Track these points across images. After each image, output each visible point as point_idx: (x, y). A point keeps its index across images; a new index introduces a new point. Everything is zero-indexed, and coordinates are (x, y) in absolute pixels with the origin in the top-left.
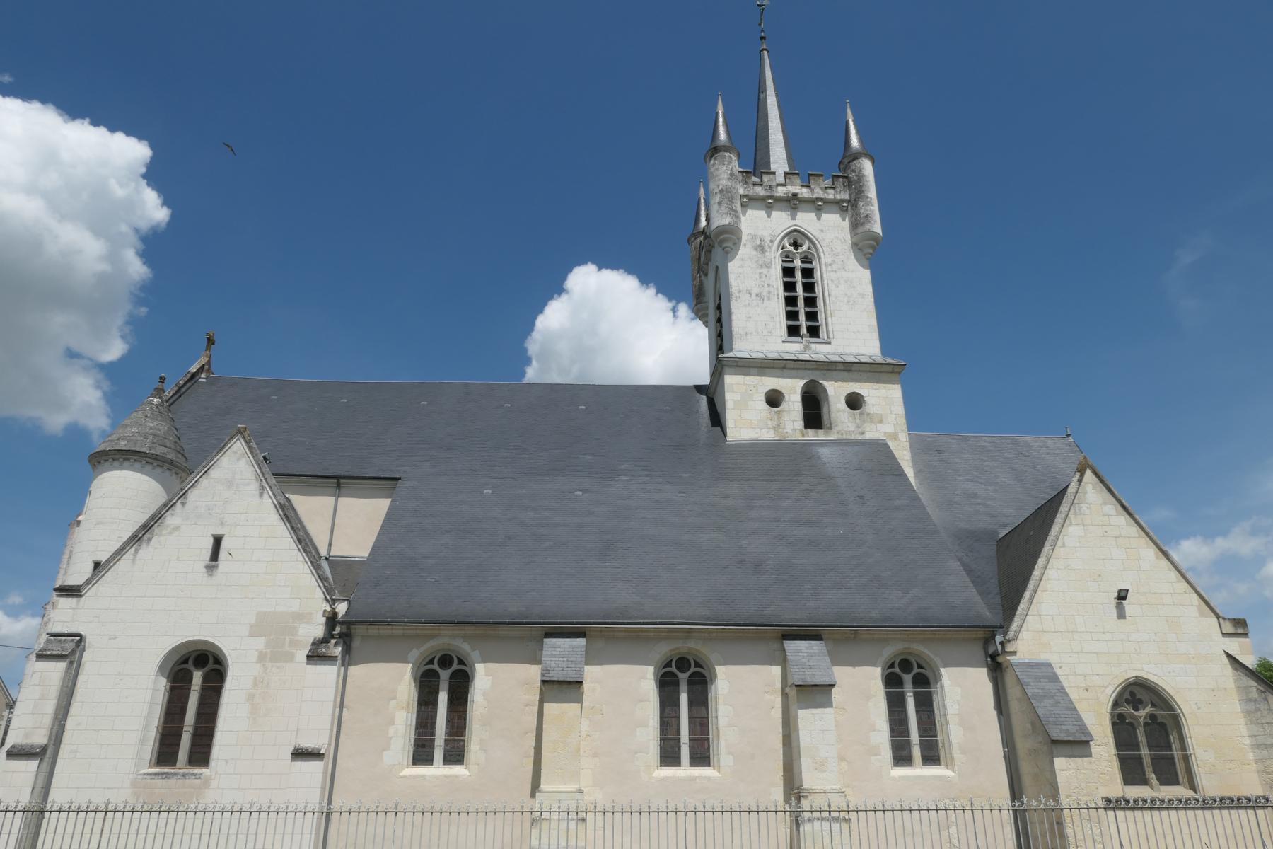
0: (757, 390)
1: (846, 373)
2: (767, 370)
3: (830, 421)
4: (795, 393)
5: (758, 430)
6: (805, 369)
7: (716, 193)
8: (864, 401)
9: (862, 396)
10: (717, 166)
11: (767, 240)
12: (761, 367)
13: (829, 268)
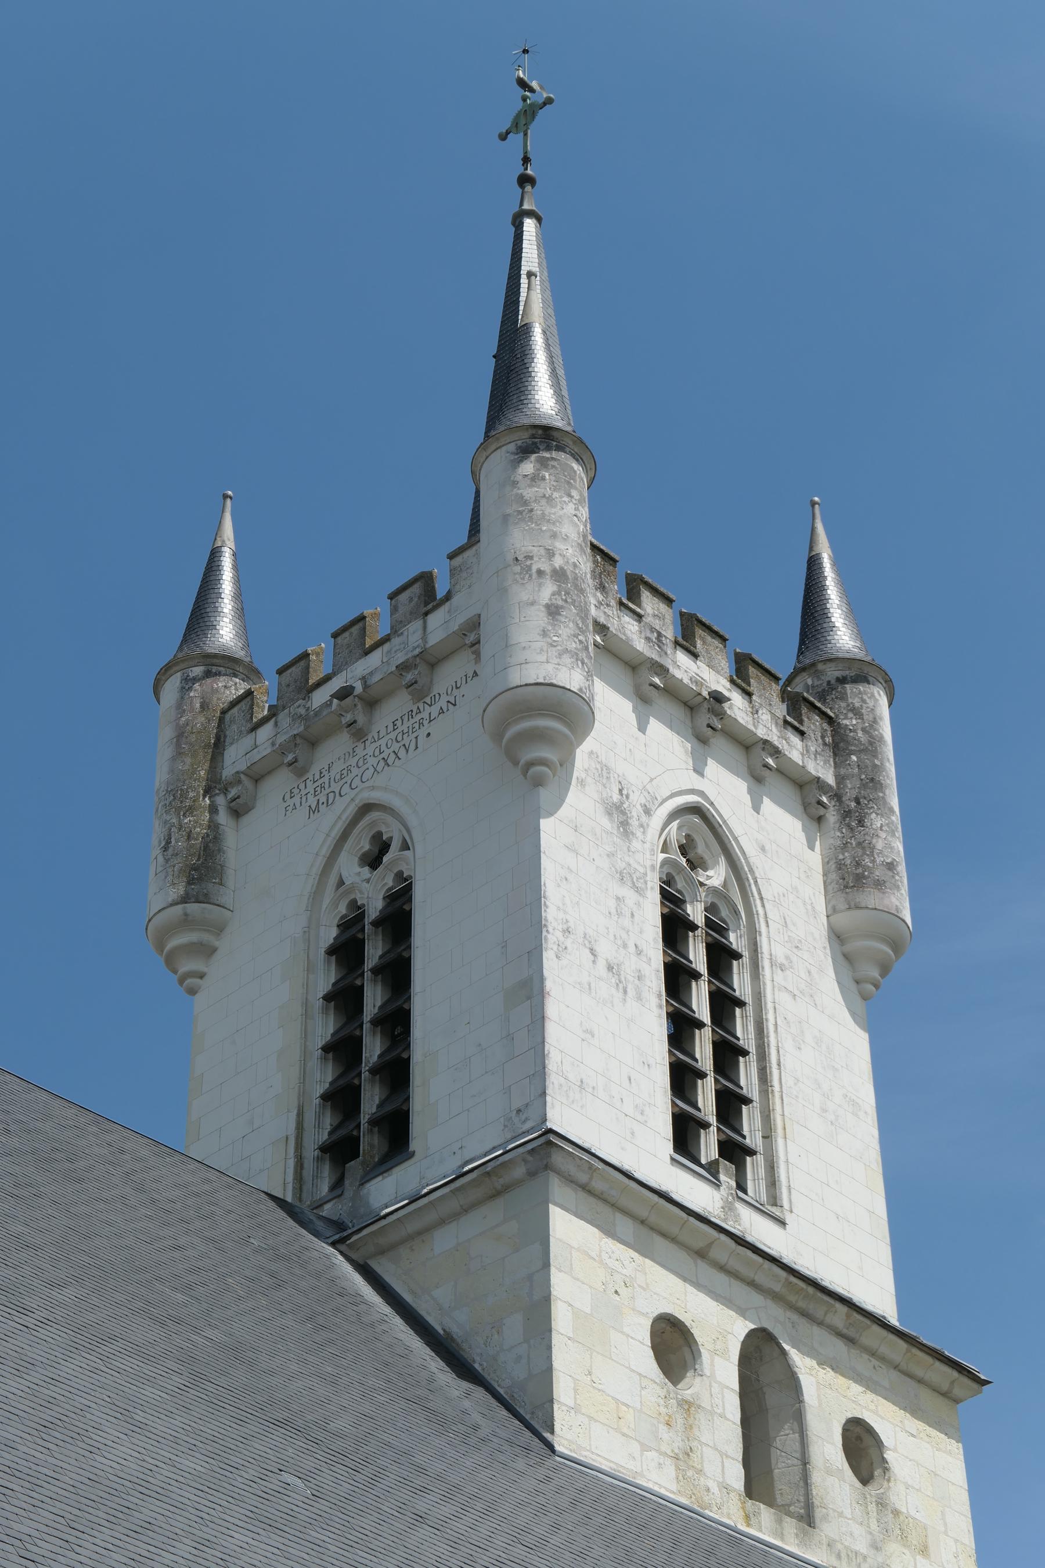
1: (840, 1345)
2: (660, 1242)
3: (808, 1494)
5: (635, 1447)
6: (752, 1284)
7: (540, 573)
8: (884, 1461)
9: (879, 1444)
10: (545, 488)
12: (643, 1222)
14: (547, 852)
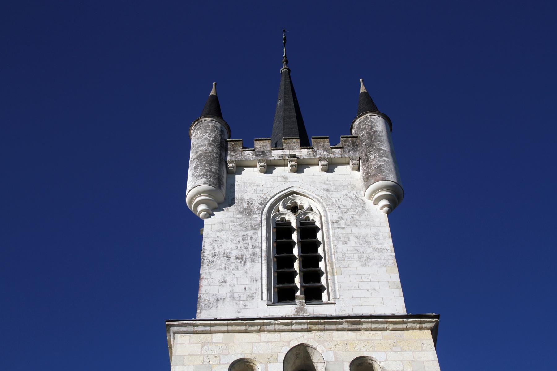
0: (220, 360)
4: (276, 360)
11: (256, 203)
13: (336, 225)
14: (206, 237)
